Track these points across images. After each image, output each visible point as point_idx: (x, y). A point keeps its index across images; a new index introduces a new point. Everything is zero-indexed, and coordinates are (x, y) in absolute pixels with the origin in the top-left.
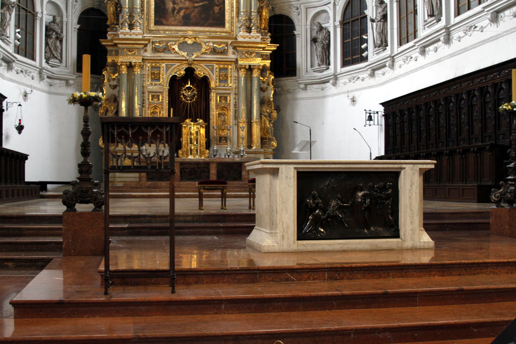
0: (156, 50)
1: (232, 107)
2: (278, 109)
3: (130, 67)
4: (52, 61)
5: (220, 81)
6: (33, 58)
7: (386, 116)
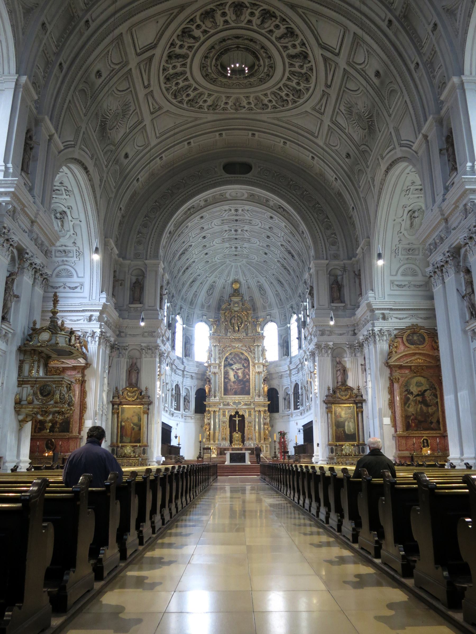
0: (224, 405)
1: (253, 426)
2: (272, 426)
3: (214, 412)
4: (186, 410)
5: (249, 416)
6: (179, 410)
7: (304, 431)
